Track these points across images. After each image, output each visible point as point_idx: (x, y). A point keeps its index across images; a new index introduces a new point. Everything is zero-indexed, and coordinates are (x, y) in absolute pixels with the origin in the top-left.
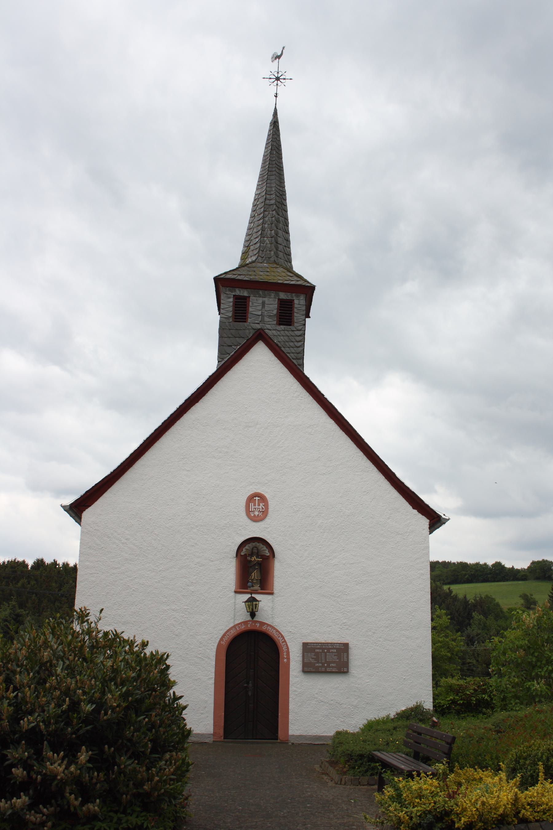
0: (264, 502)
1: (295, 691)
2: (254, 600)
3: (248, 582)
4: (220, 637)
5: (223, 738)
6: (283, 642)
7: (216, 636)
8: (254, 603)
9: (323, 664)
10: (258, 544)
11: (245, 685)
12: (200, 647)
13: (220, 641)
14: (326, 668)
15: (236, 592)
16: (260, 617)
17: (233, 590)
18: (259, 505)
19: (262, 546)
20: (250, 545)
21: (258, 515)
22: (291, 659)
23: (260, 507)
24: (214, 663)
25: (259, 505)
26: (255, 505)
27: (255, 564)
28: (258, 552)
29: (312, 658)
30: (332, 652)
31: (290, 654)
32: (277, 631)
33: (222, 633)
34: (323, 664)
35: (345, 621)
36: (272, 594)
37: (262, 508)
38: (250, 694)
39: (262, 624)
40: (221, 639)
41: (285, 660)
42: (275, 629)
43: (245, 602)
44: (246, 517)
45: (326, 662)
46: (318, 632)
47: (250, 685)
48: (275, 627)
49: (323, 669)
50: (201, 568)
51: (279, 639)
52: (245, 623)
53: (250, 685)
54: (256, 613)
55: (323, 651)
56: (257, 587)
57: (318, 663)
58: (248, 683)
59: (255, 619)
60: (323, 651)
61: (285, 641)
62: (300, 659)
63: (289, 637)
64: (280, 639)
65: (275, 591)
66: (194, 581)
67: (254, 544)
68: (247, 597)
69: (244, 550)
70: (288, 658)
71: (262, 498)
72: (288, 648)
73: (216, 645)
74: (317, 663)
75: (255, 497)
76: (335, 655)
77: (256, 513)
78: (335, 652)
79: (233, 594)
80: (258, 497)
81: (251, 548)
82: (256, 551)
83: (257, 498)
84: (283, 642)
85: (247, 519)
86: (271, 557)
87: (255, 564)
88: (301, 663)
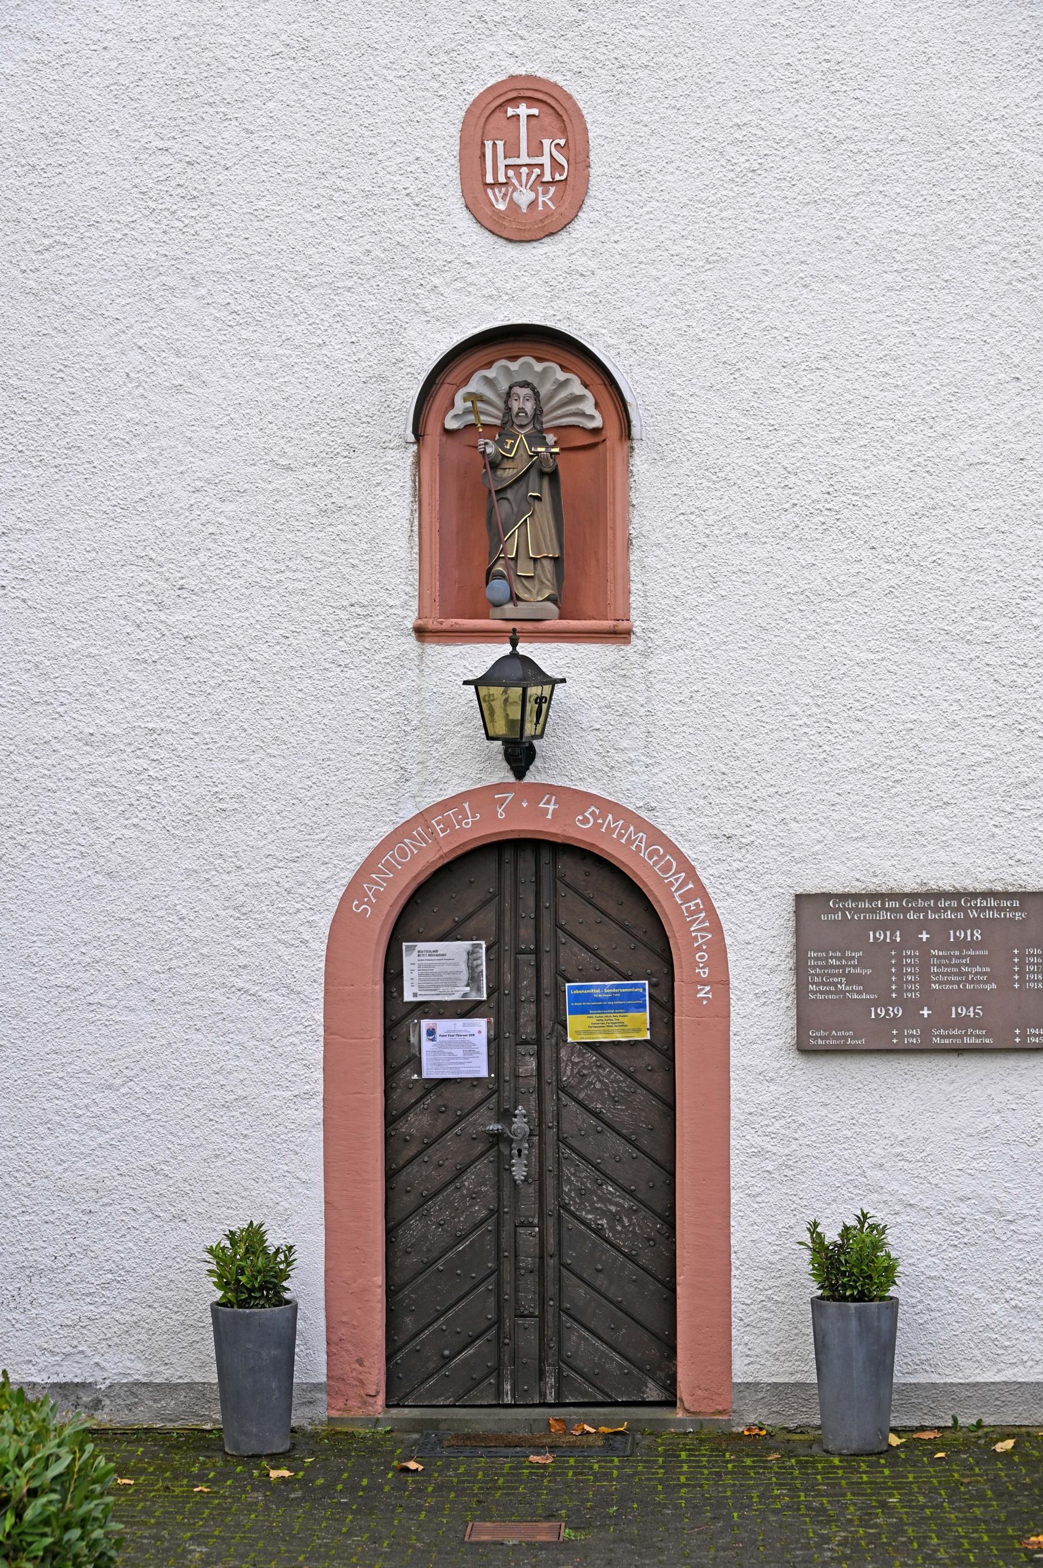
0: (564, 131)
1: (760, 1153)
2: (528, 672)
3: (490, 575)
4: (347, 877)
5: (381, 1400)
6: (686, 897)
7: (322, 874)
8: (534, 691)
9: (911, 1007)
10: (539, 367)
11: (494, 1127)
12: (238, 935)
13: (345, 900)
14: (926, 1027)
15: (421, 633)
16: (568, 759)
17: (409, 624)
18: (536, 149)
19: (562, 376)
20: (491, 373)
21: (533, 204)
22: (733, 983)
23: (546, 160)
24: (320, 1017)
25: (536, 149)
26: (512, 150)
27: (522, 479)
28: (538, 413)
29: (851, 979)
30: (960, 944)
31: (731, 957)
32: (657, 836)
33: (359, 853)
34: (911, 1007)
35: (1026, 774)
36: (621, 635)
37: (556, 165)
38: (519, 1172)
39: (574, 800)
40: (353, 890)
41: (704, 992)
42: (642, 825)
43: (476, 683)
44: (464, 221)
45: (928, 997)
46: (880, 836)
47: (520, 1124)
48: (643, 814)
49: (913, 1037)
50: (228, 508)
51: (669, 878)
52: (479, 797)
53: (520, 1124)
54: (535, 742)
55: (910, 940)
56: (536, 601)
57: (885, 1001)
58: (506, 1115)
59: (529, 778)
60: (910, 940)
61: (701, 891)
62: (784, 980)
63: (722, 868)
64: (676, 879)
65: (637, 624)
66: (192, 583)
67: (514, 366)
68: (486, 655)
69: (460, 405)
70: (721, 983)
71: (554, 109)
72: (716, 927)
73: (325, 922)
74: (876, 1004)
75: (514, 101)
76: (975, 961)
77: (524, 197)
78: (974, 944)
79: (411, 642)
80: (531, 101)
81: (504, 386)
82: (529, 407)
83: (523, 110)
84: (686, 897)
85: (475, 227)
86: (612, 433)
87: (522, 479)
88: (790, 1002)
